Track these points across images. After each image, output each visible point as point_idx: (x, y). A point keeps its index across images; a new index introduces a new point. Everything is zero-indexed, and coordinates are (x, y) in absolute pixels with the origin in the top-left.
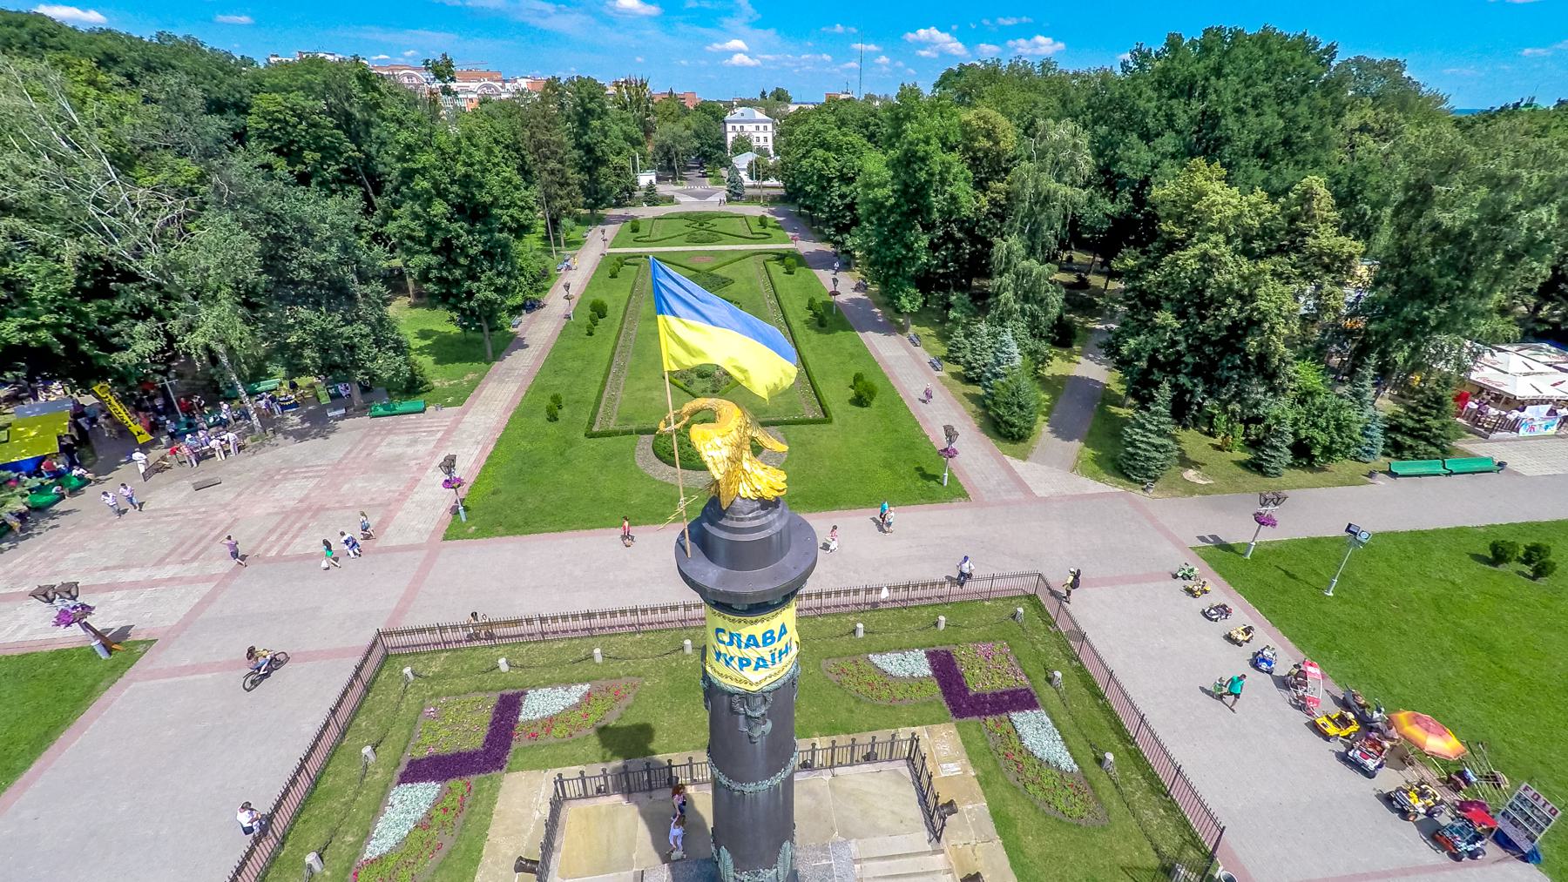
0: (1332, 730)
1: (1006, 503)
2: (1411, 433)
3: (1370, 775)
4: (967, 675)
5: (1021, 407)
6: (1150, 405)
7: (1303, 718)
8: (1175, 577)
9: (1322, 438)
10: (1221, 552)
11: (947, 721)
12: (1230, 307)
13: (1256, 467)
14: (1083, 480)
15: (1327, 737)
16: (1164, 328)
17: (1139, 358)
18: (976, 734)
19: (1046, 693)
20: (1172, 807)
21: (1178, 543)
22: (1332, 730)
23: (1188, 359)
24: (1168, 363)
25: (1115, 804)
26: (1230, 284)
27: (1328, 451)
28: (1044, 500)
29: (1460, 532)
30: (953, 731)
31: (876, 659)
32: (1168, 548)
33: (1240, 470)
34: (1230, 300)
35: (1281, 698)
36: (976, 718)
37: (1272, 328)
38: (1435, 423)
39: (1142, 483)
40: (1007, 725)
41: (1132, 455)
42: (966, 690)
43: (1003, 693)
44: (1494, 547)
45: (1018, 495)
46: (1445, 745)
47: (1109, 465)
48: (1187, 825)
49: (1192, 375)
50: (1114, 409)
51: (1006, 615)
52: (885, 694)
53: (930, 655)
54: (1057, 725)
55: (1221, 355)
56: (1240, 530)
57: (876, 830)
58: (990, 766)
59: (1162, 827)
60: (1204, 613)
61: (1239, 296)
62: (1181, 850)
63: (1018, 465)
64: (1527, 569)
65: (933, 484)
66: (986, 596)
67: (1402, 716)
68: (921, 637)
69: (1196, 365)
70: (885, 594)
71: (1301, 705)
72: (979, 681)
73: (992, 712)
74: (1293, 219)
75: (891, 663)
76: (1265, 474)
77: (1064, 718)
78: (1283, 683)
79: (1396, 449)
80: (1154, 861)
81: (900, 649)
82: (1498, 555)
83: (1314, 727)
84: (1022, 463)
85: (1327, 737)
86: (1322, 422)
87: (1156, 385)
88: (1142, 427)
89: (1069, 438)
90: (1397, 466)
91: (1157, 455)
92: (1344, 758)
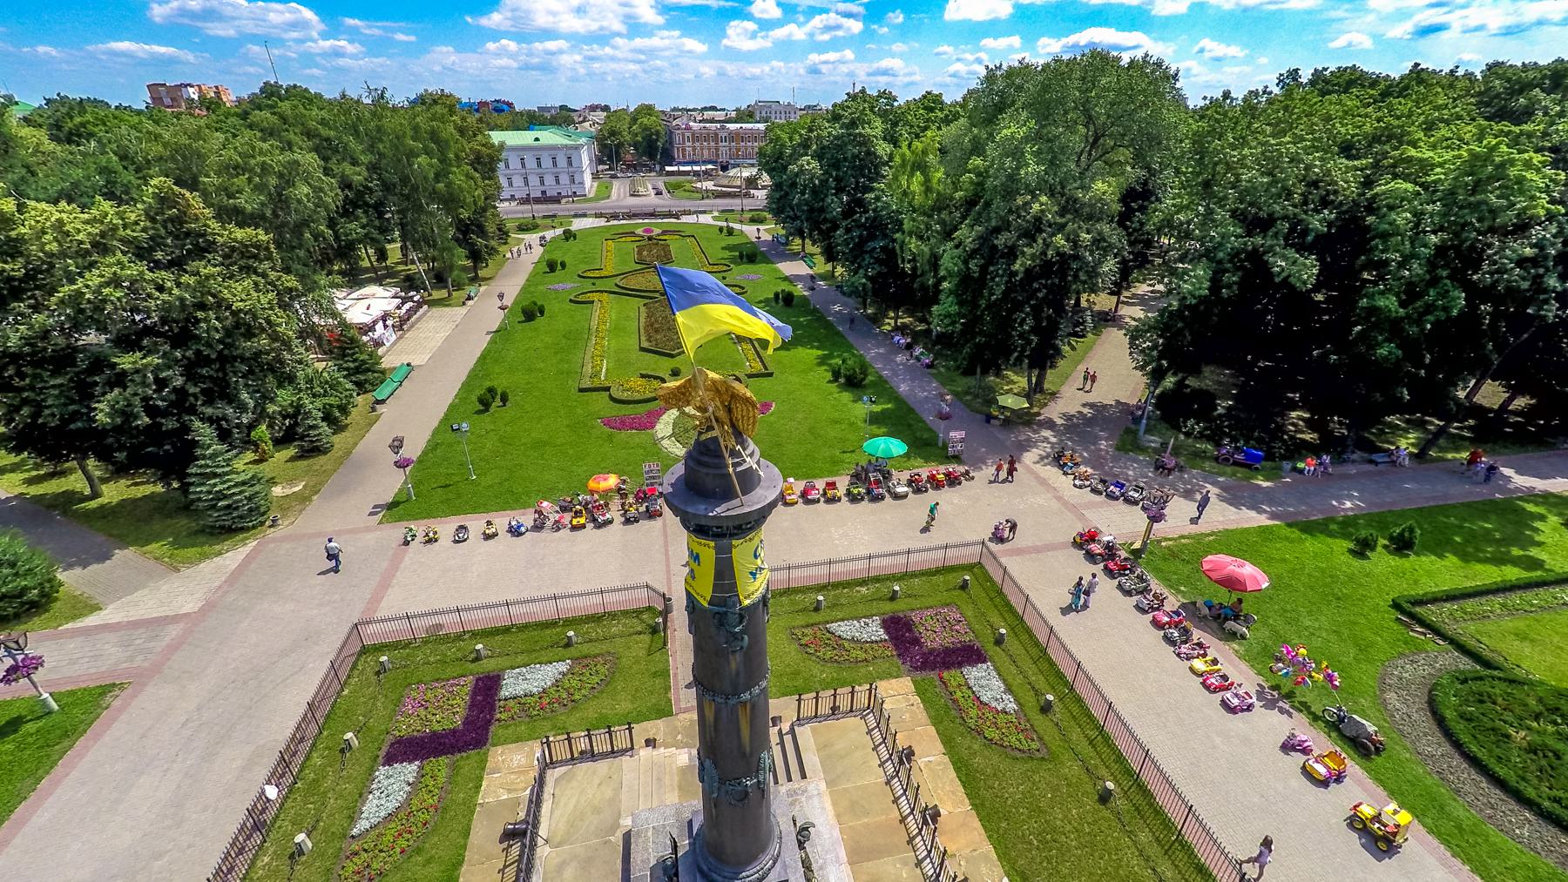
0: (582, 521)
1: (174, 647)
2: (357, 371)
3: (611, 522)
4: (437, 727)
5: (13, 565)
6: (199, 452)
7: (565, 533)
8: (406, 543)
9: (332, 400)
10: (394, 509)
11: (486, 754)
12: (206, 320)
13: (313, 450)
14: (206, 567)
15: (584, 526)
16: (137, 371)
17: (136, 417)
18: (510, 731)
19: (488, 666)
20: (613, 615)
21: (367, 529)
22: (582, 521)
23: (192, 390)
24: (172, 404)
25: (605, 647)
26: (182, 300)
27: (344, 409)
28: (208, 607)
29: (452, 407)
30: (500, 749)
31: (363, 825)
32: (371, 538)
33: (303, 464)
34: (200, 314)
35: (545, 535)
36: (492, 728)
37: (269, 322)
38: (364, 357)
39: (262, 524)
40: (511, 703)
41: (228, 507)
42: (454, 731)
43: (473, 698)
44: (481, 401)
45: (174, 631)
46: (612, 481)
47: (202, 539)
48: (625, 613)
49: (209, 402)
50: (93, 504)
51: (373, 678)
52: (423, 817)
53: (390, 760)
54: (525, 666)
55: (222, 369)
56: (391, 483)
57: (614, 801)
58: (548, 724)
59: (625, 625)
60: (456, 542)
61: (202, 306)
62: (643, 621)
63: (92, 620)
64: (498, 402)
65: (30, 727)
66: (336, 686)
67: (592, 485)
68: (355, 770)
69: (203, 391)
70: (272, 792)
71: (557, 526)
72: (451, 715)
73: (492, 709)
74: (179, 220)
75: (374, 809)
76: (325, 452)
77: (520, 659)
78: (538, 527)
79: (361, 387)
80: (646, 638)
81: (362, 796)
82: (485, 404)
83: (574, 528)
84: (103, 613)
85: (584, 526)
86: (318, 389)
87: (186, 429)
88: (215, 475)
89: (104, 557)
90: (381, 393)
91: (257, 488)
92: (599, 526)
